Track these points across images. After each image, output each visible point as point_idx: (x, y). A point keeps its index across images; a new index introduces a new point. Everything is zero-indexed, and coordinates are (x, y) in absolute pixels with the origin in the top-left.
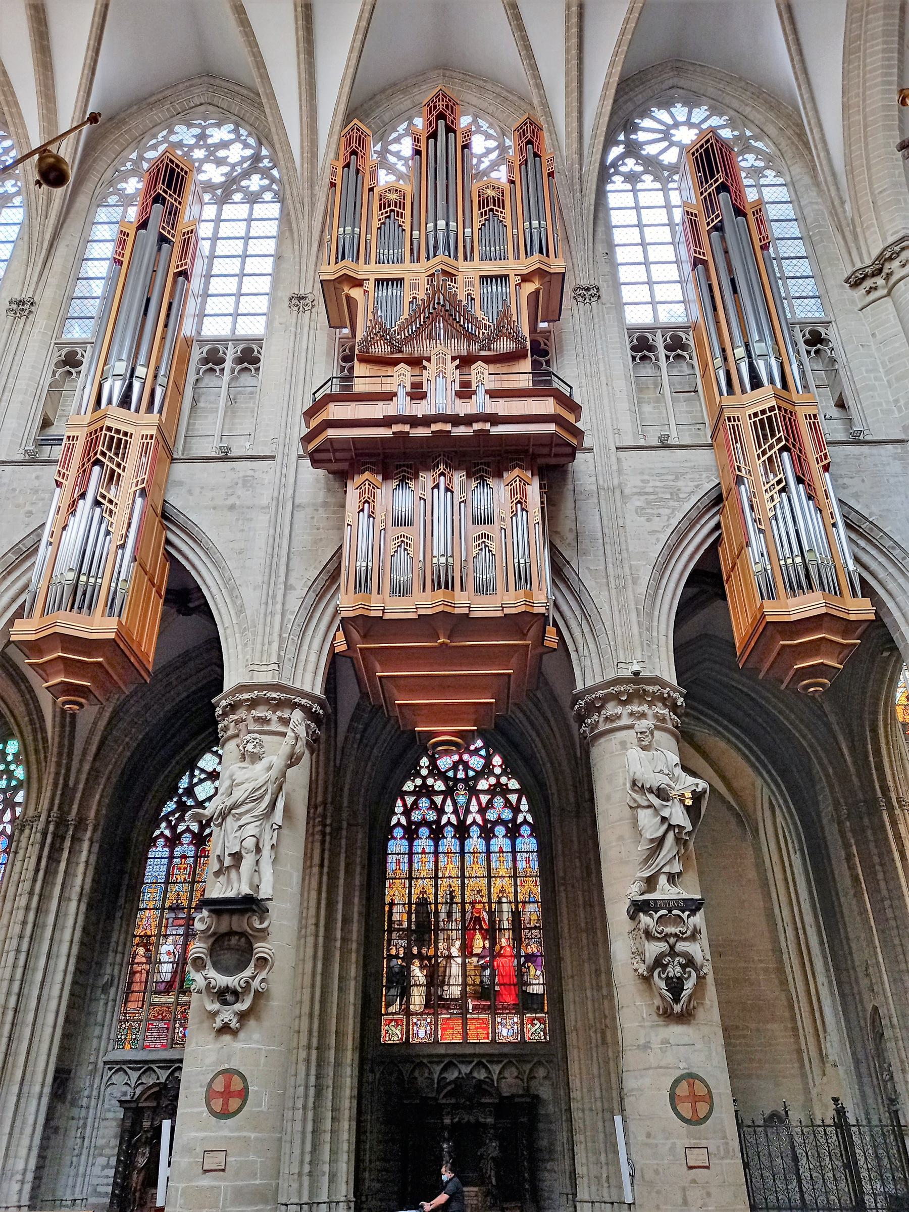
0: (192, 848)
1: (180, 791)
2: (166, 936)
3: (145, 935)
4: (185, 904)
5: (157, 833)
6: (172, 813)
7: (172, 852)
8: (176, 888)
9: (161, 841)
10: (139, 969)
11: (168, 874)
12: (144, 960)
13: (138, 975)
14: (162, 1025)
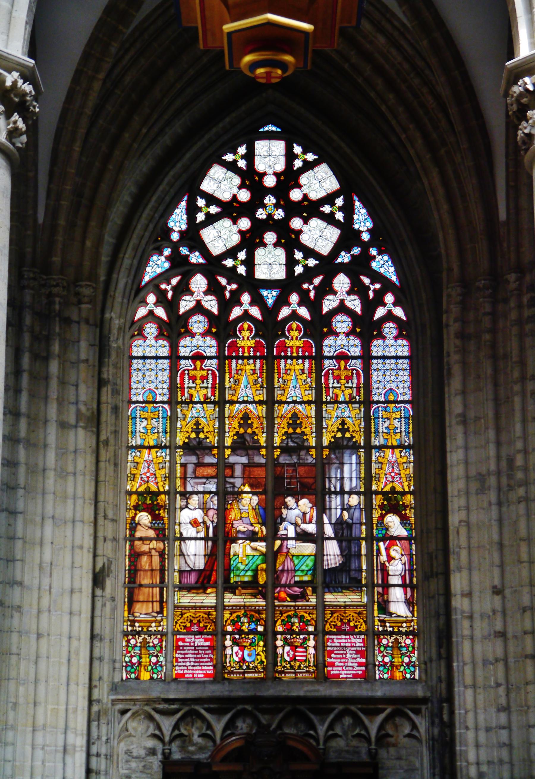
0: (211, 341)
1: (175, 237)
2: (185, 495)
3: (148, 492)
4: (214, 440)
5: (142, 312)
6: (165, 276)
7: (174, 348)
8: (195, 411)
9: (151, 329)
10: (145, 548)
11: (173, 388)
12: (151, 533)
13: (144, 559)
14: (200, 641)
